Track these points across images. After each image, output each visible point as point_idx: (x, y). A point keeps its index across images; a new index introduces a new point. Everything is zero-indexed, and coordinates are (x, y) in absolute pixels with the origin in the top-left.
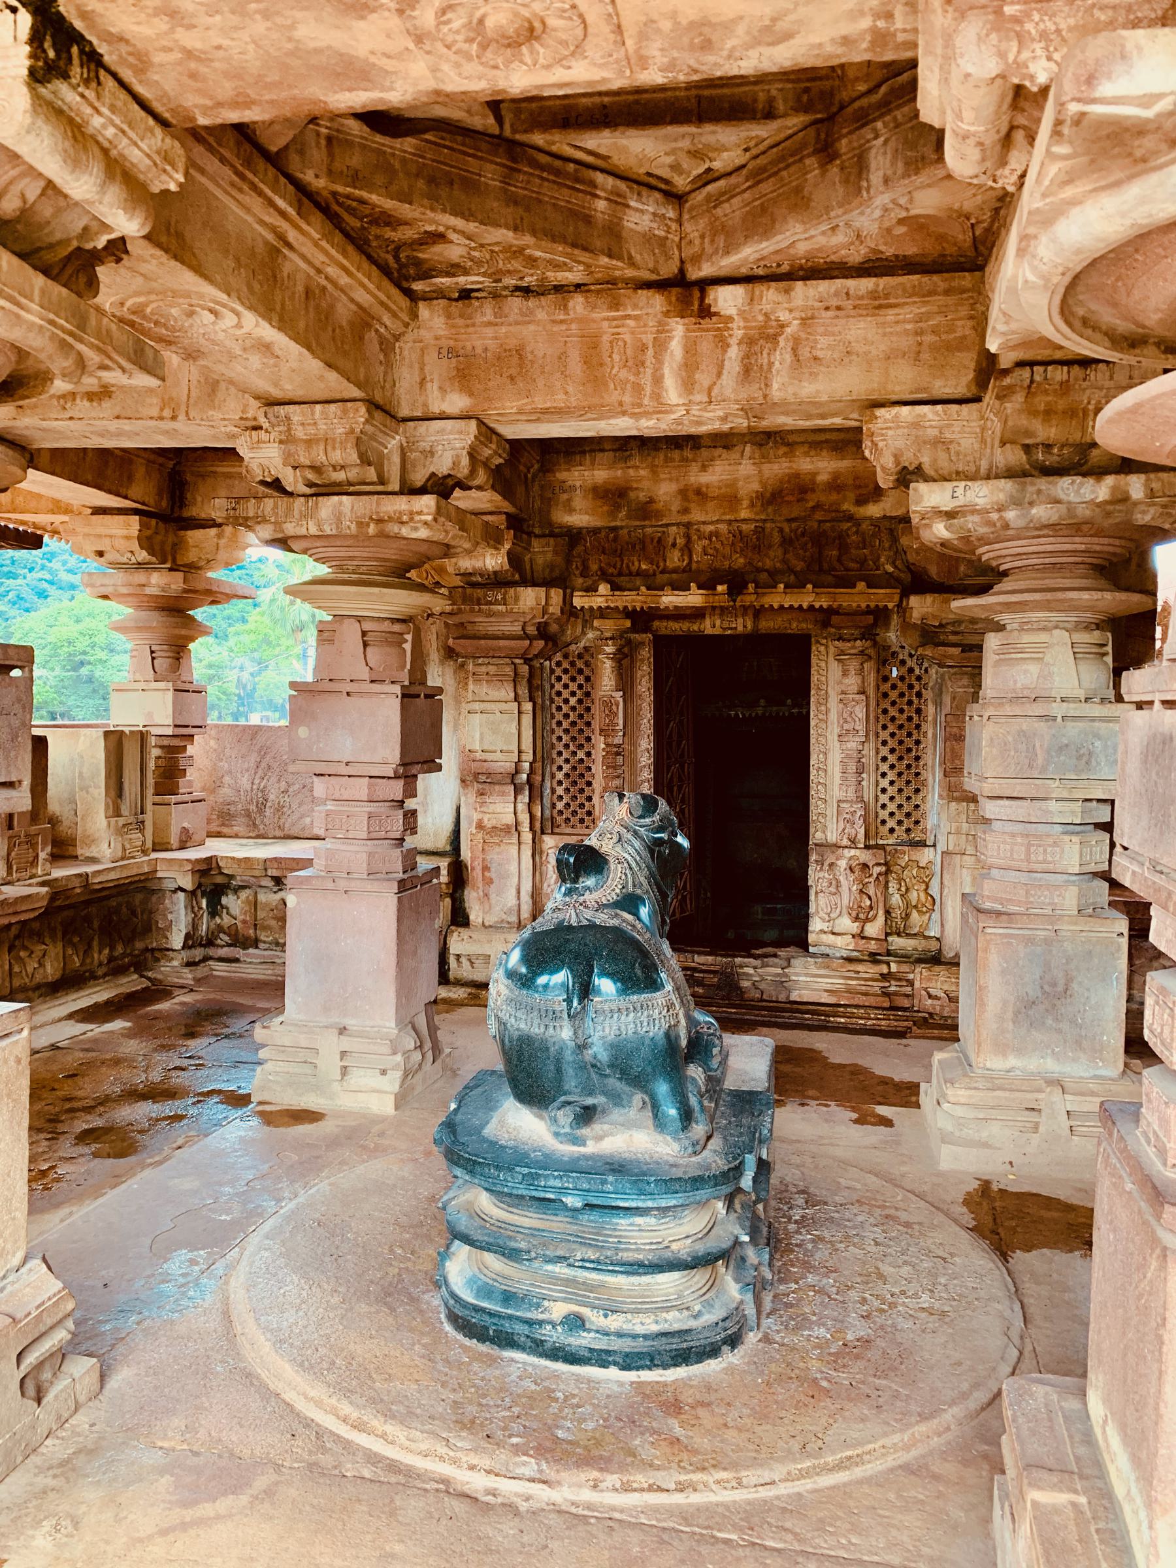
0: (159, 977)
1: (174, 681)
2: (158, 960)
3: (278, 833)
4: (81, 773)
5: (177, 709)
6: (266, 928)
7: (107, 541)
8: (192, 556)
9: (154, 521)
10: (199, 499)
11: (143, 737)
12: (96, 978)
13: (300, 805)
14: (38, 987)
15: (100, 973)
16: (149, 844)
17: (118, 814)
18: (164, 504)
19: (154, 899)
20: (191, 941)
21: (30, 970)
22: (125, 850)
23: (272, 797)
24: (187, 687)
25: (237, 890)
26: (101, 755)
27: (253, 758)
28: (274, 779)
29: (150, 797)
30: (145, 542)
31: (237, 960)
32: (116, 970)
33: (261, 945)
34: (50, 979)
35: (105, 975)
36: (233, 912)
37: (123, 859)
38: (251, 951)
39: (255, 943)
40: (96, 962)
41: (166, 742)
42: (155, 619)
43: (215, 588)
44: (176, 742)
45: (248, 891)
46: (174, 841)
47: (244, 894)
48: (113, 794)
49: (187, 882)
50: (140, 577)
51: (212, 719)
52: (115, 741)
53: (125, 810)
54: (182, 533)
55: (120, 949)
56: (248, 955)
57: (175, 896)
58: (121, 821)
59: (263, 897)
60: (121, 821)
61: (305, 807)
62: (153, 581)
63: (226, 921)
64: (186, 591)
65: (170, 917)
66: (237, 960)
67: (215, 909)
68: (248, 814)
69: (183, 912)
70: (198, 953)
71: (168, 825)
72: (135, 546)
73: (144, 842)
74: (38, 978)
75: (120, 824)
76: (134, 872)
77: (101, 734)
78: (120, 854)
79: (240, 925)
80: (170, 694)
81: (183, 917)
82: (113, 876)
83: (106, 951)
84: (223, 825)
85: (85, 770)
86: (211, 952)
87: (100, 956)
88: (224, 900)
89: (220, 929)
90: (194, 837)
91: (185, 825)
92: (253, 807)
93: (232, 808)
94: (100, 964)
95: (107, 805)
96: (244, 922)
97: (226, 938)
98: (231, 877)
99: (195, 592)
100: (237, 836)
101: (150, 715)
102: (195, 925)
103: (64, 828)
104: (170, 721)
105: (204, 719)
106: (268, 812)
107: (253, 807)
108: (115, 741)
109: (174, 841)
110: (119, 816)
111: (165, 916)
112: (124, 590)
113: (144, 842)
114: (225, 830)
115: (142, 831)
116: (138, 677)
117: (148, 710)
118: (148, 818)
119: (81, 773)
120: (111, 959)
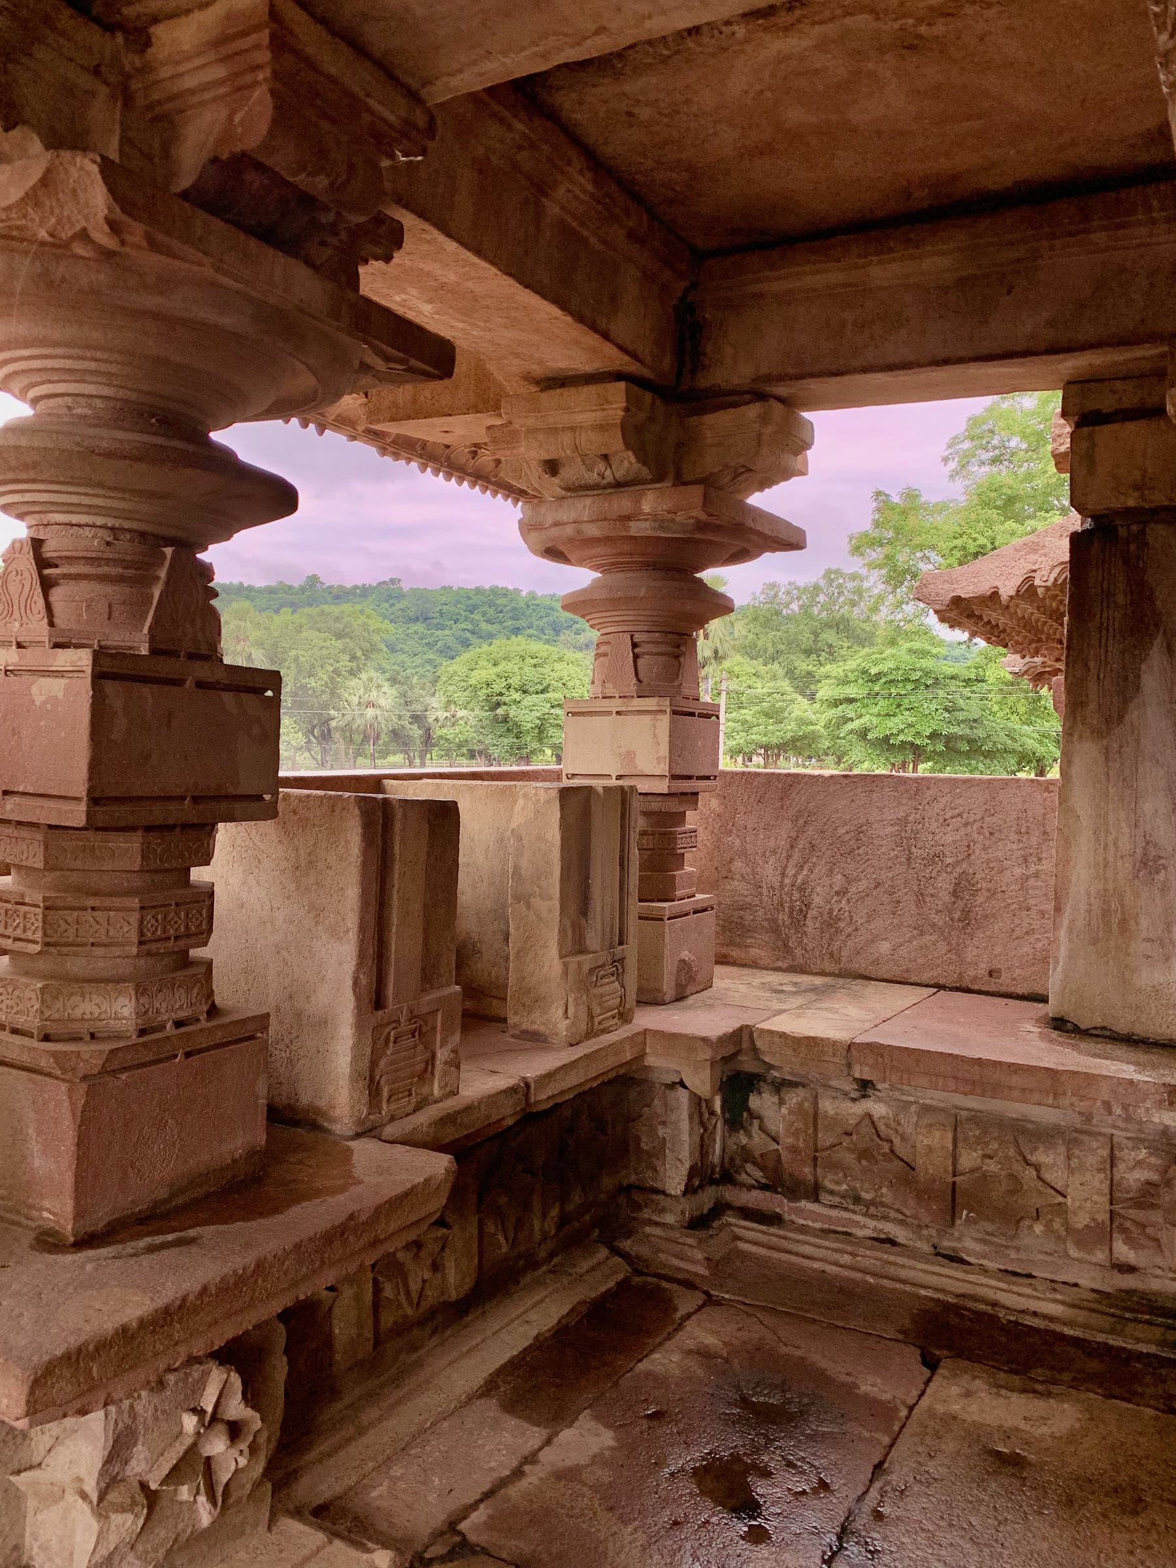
0: (645, 1251)
1: (672, 698)
2: (638, 1207)
3: (829, 966)
4: (517, 868)
5: (678, 745)
6: (834, 1166)
7: (566, 438)
8: (710, 462)
9: (648, 397)
10: (728, 350)
11: (623, 796)
12: (533, 1265)
13: (870, 918)
14: (432, 1313)
15: (543, 1254)
16: (632, 997)
17: (580, 948)
18: (667, 363)
19: (633, 1094)
20: (702, 1176)
21: (415, 1286)
22: (591, 1017)
23: (817, 900)
24: (690, 706)
25: (780, 1086)
26: (554, 834)
27: (785, 829)
28: (821, 869)
29: (635, 907)
30: (634, 434)
31: (774, 1219)
32: (572, 1241)
33: (825, 1198)
34: (454, 1295)
35: (552, 1255)
36: (771, 1126)
37: (590, 1034)
38: (803, 1204)
39: (814, 1192)
40: (537, 1235)
41: (655, 805)
42: (641, 585)
43: (750, 523)
44: (673, 806)
45: (801, 1092)
46: (668, 987)
47: (794, 1098)
48: (573, 910)
49: (701, 1081)
50: (622, 503)
51: (725, 764)
52: (577, 803)
53: (593, 940)
54: (694, 420)
55: (577, 1198)
56: (800, 1212)
57: (672, 1095)
58: (587, 960)
59: (827, 1106)
60: (587, 960)
61: (878, 924)
62: (646, 508)
63: (757, 1141)
64: (701, 526)
65: (661, 1131)
66: (774, 1219)
67: (737, 1114)
68: (775, 930)
69: (685, 1125)
70: (707, 1198)
71: (659, 958)
72: (616, 443)
73: (623, 998)
74: (432, 1296)
75: (586, 968)
76: (611, 1062)
77: (554, 794)
78: (583, 1027)
79: (785, 1155)
80: (665, 721)
81: (685, 1137)
82: (573, 1079)
83: (555, 1212)
84: (731, 943)
85: (524, 863)
86: (730, 1194)
87: (542, 1224)
88: (754, 1102)
89: (746, 1155)
90: (699, 978)
91: (685, 955)
92: (783, 917)
93: (748, 917)
94: (545, 1237)
95: (562, 931)
96: (794, 1149)
97: (758, 1174)
98: (771, 1067)
99: (717, 528)
100: (754, 965)
101: (630, 756)
102: (703, 1148)
103: (482, 968)
104: (663, 768)
105: (715, 763)
106: (811, 926)
107: (783, 917)
108: (577, 803)
109: (668, 987)
110: (583, 951)
111: (653, 1129)
112: (593, 531)
113: (623, 998)
114: (735, 953)
115: (619, 975)
116: (610, 690)
117: (626, 749)
118: (630, 950)
119: (517, 868)
120: (564, 1220)
